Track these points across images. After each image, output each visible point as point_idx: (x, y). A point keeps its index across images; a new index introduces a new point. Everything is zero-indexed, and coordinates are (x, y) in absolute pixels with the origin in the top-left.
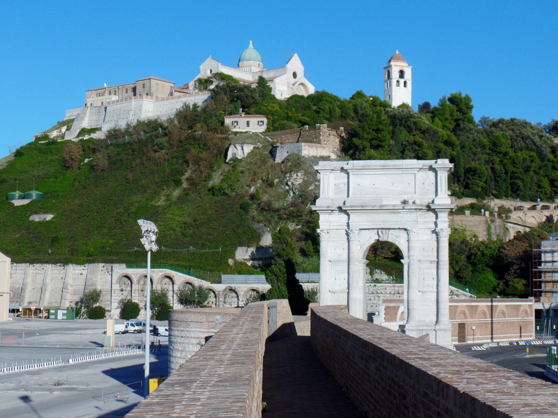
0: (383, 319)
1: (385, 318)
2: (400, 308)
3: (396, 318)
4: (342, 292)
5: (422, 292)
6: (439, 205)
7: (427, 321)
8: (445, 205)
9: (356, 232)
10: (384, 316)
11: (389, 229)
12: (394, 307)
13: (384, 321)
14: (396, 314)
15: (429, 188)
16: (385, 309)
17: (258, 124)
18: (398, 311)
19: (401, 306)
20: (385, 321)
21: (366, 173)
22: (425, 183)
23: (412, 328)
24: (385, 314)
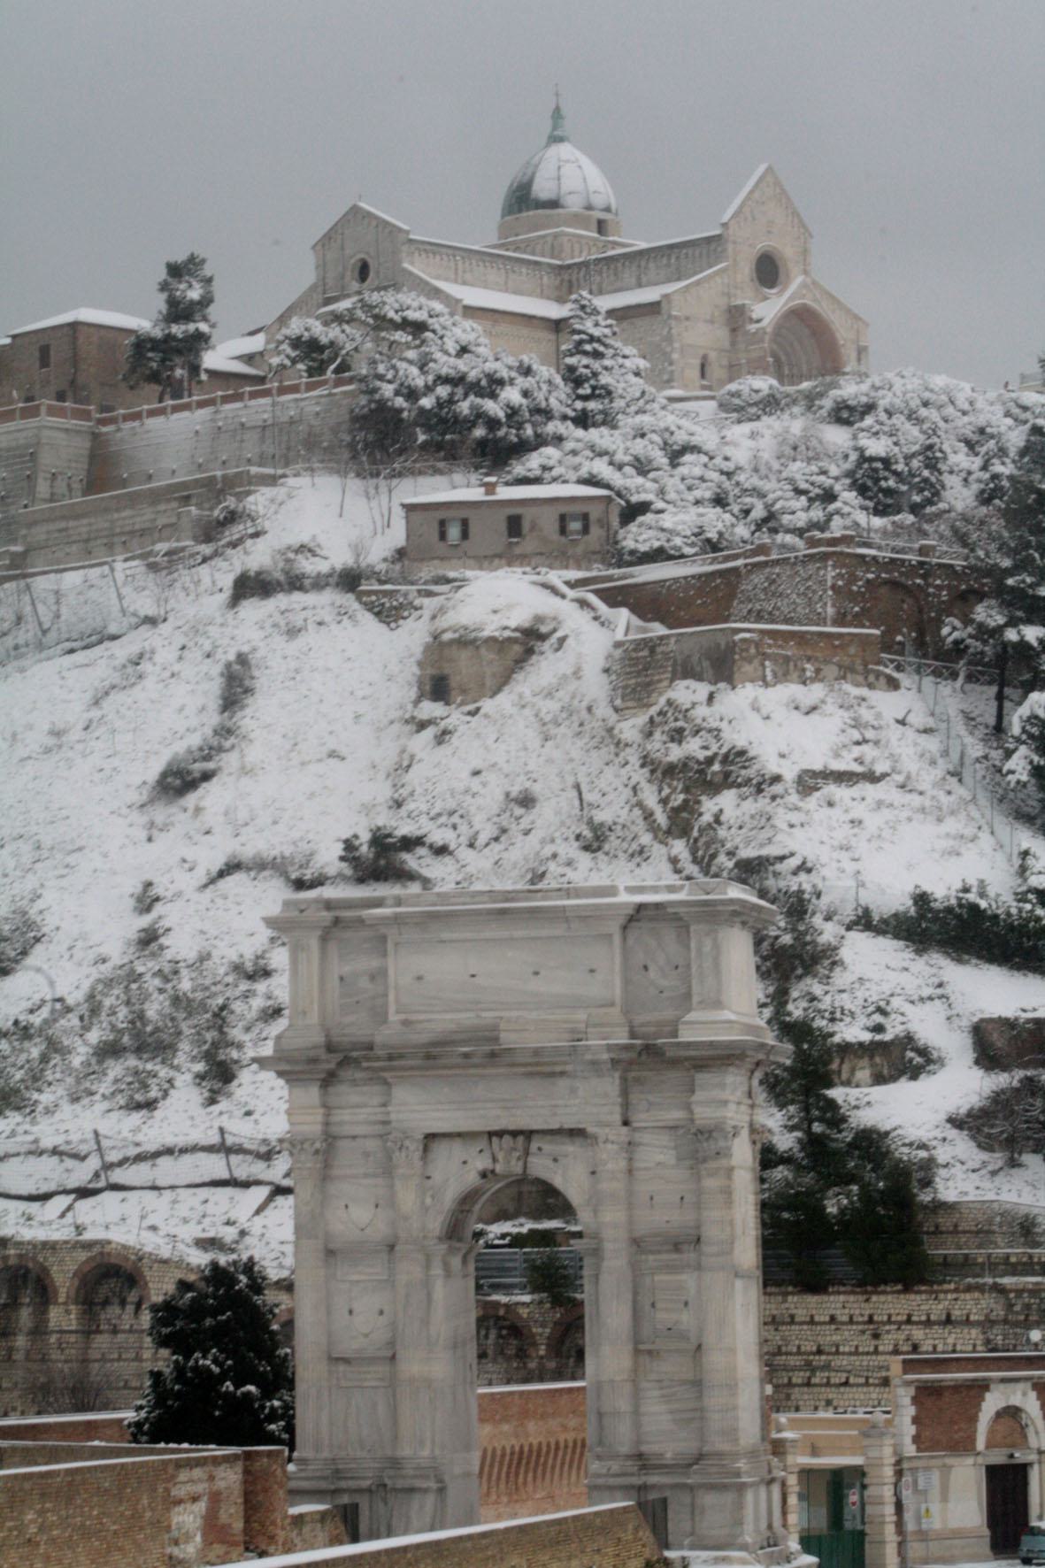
0: (908, 1440)
1: (916, 1439)
2: (988, 1396)
3: (972, 1439)
4: (373, 1360)
5: (650, 1352)
6: (689, 1045)
7: (669, 1455)
8: (711, 1044)
9: (415, 1148)
10: (912, 1430)
11: (528, 1135)
12: (957, 1388)
13: (910, 1449)
14: (973, 1419)
15: (664, 983)
16: (916, 1400)
17: (563, 531)
18: (978, 1407)
19: (992, 1386)
20: (919, 1450)
21: (446, 935)
22: (649, 964)
23: (611, 1481)
24: (915, 1420)
